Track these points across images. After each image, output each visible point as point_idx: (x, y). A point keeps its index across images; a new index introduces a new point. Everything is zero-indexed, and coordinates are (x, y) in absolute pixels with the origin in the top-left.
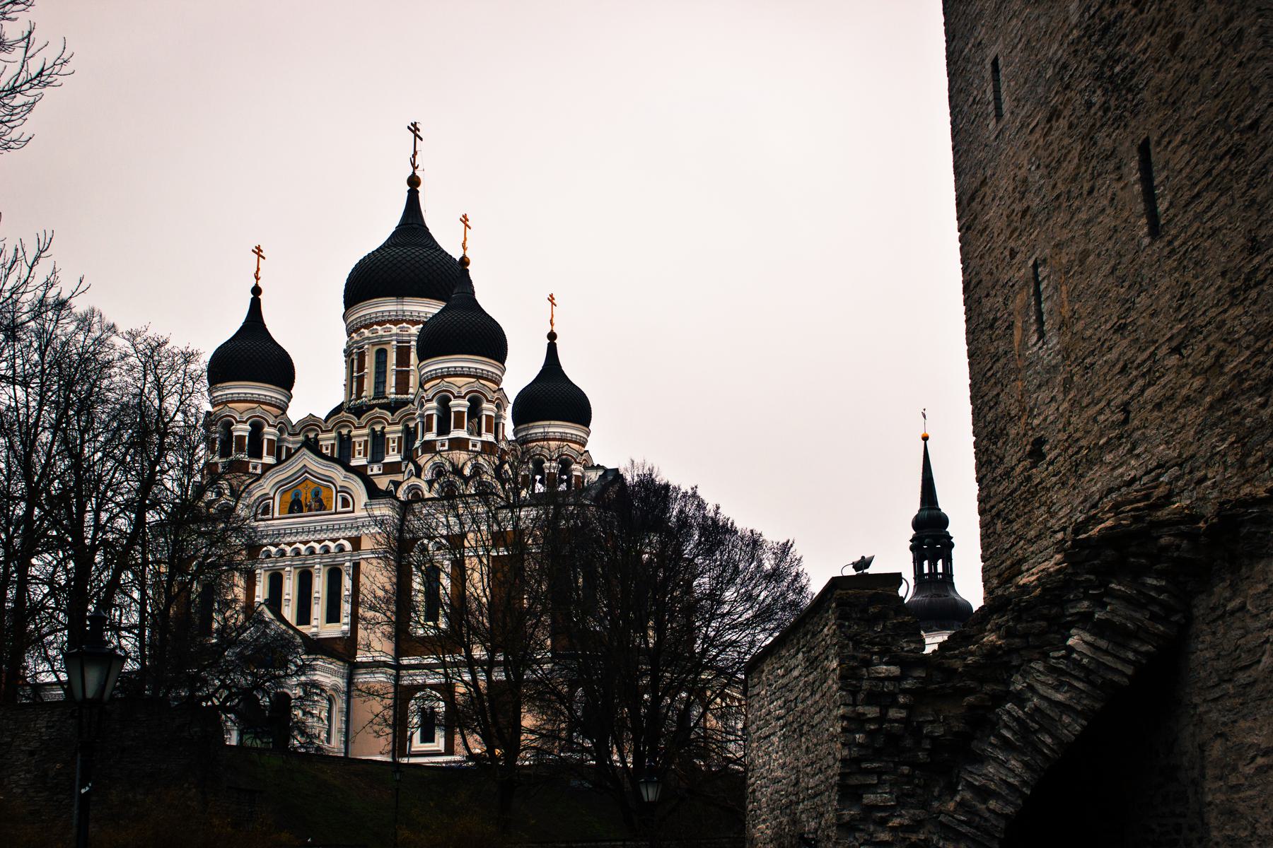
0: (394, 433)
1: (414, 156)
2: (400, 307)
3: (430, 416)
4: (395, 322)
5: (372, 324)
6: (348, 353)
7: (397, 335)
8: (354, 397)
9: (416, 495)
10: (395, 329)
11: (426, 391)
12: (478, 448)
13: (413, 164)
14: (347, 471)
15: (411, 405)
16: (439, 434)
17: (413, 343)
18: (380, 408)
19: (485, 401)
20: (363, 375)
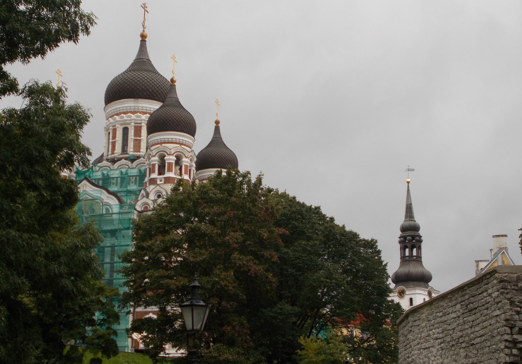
3: (154, 165)
4: (134, 113)
5: (120, 114)
6: (107, 129)
7: (134, 119)
8: (110, 153)
9: (146, 207)
10: (133, 116)
11: (152, 151)
13: (143, 26)
15: (142, 158)
16: (160, 174)
20: (115, 142)
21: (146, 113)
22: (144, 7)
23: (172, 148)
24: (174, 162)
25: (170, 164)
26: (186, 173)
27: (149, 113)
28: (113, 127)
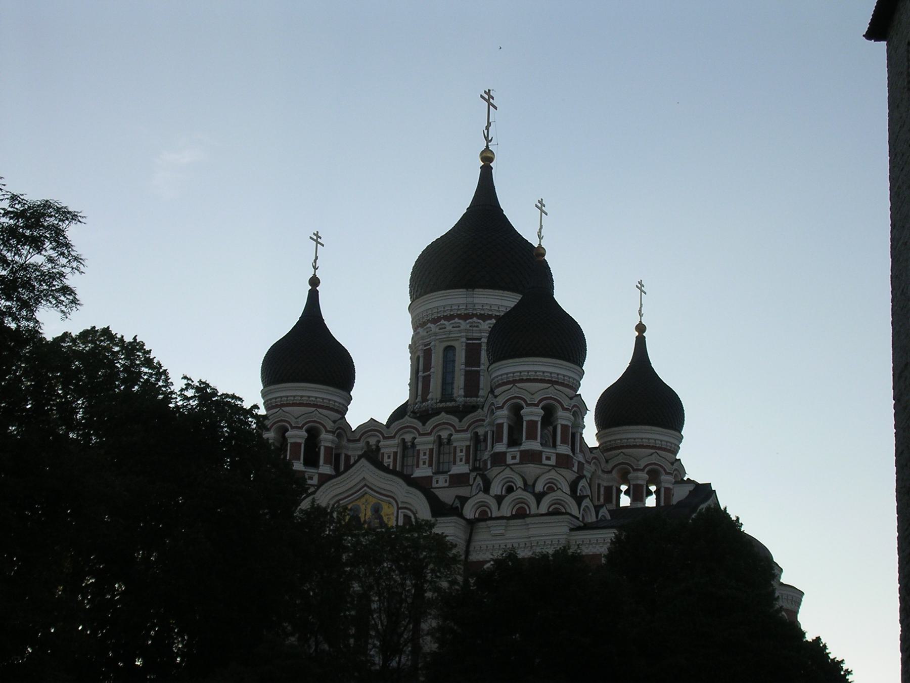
0: (462, 440)
1: (487, 128)
2: (470, 300)
3: (500, 426)
4: (466, 317)
7: (467, 331)
8: (419, 399)
9: (484, 513)
10: (464, 325)
11: (496, 397)
12: (553, 462)
13: (486, 138)
15: (480, 410)
17: (485, 340)
19: (560, 409)
20: (429, 376)
21: (490, 317)
22: (488, 97)
23: (537, 391)
24: (539, 419)
25: (532, 424)
26: (564, 441)
27: (496, 317)
28: (425, 346)
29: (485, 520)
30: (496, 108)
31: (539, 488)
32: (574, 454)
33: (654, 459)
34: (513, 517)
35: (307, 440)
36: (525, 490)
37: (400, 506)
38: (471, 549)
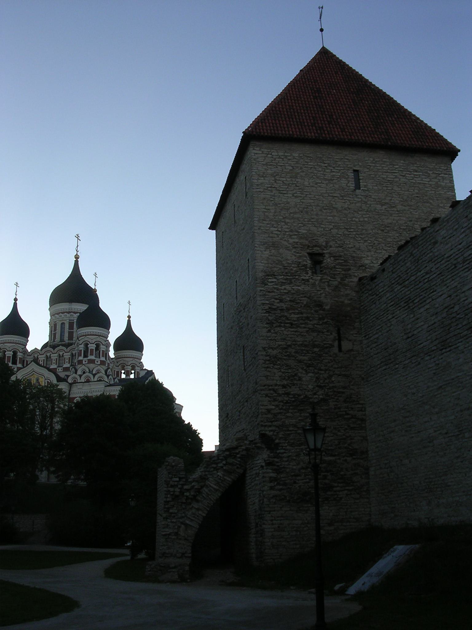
0: (67, 356)
1: (77, 247)
4: (69, 313)
7: (69, 317)
8: (52, 341)
10: (68, 315)
11: (79, 340)
12: (99, 363)
13: (77, 251)
14: (49, 371)
15: (73, 345)
17: (75, 321)
18: (62, 346)
20: (56, 333)
21: (77, 313)
22: (78, 237)
23: (93, 339)
24: (94, 348)
25: (92, 350)
26: (103, 356)
27: (79, 313)
29: (75, 383)
30: (80, 240)
31: (94, 372)
32: (106, 360)
33: (133, 362)
34: (85, 382)
35: (13, 355)
36: (89, 373)
37: (46, 378)
38: (71, 393)
